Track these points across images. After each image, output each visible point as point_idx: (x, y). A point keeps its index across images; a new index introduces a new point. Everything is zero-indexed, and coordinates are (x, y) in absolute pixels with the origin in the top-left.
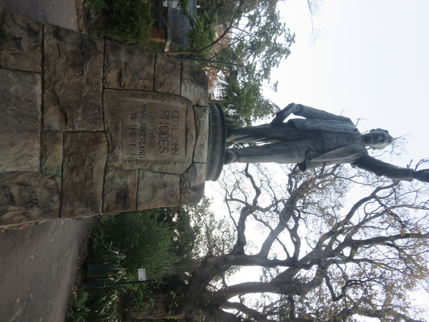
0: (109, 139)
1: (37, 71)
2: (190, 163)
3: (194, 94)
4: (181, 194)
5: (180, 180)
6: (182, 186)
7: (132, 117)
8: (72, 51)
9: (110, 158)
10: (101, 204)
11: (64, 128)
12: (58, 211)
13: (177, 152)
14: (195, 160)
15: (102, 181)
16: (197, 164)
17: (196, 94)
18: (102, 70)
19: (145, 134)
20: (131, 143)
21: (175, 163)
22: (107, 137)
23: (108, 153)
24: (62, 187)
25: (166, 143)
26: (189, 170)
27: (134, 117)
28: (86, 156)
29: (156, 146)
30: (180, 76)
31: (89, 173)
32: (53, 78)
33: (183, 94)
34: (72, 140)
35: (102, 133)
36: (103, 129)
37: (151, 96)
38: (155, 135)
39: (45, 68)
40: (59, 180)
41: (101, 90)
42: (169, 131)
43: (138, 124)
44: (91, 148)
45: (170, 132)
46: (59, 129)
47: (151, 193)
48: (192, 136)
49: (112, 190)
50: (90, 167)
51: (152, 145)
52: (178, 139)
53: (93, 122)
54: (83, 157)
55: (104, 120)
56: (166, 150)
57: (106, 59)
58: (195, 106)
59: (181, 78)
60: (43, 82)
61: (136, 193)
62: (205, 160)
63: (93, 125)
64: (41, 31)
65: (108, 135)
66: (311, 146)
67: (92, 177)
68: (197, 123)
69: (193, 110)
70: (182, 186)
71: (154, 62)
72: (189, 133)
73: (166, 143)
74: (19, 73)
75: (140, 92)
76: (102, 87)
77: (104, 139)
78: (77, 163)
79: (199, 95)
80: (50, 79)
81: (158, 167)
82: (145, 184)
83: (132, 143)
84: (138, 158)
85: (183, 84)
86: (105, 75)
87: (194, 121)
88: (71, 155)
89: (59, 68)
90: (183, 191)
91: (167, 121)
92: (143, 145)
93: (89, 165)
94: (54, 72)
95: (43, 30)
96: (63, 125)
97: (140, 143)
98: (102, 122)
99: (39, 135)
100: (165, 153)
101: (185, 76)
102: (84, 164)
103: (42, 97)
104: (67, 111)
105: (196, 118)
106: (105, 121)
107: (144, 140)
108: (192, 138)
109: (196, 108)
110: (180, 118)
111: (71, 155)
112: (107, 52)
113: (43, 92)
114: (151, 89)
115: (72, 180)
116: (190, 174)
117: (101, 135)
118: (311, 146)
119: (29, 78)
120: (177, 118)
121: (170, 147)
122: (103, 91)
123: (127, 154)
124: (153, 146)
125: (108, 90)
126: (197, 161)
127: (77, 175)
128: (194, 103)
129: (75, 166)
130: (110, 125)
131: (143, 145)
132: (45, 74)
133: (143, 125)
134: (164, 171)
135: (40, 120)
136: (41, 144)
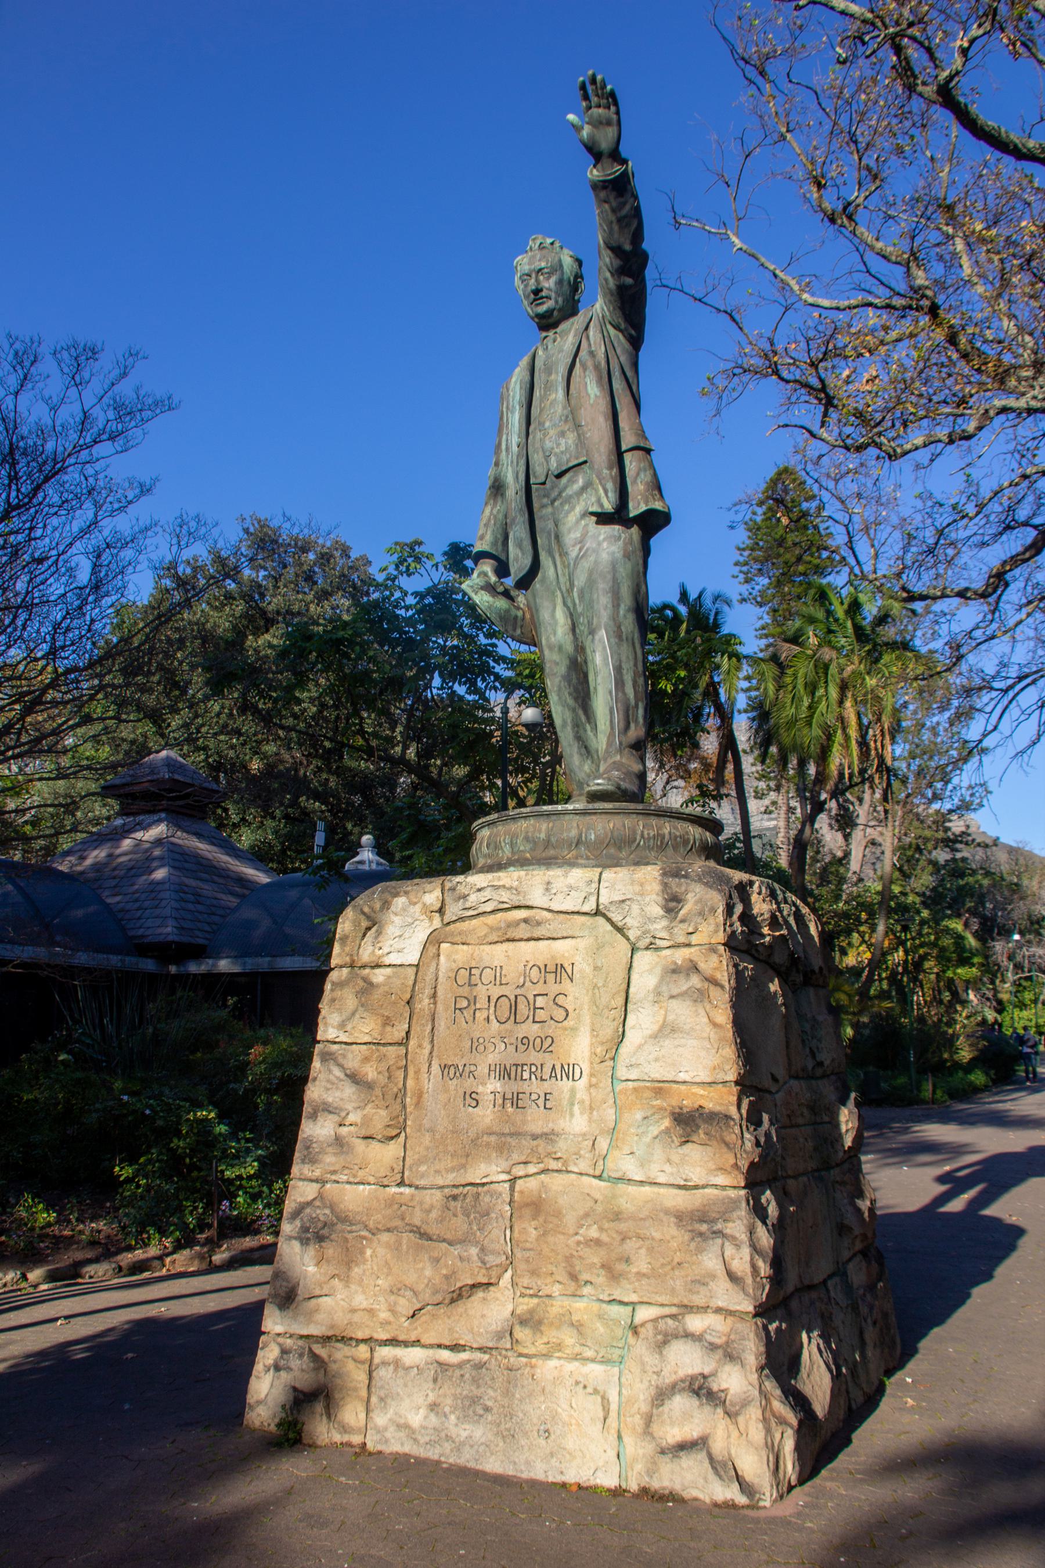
0: (532, 1169)
1: (368, 1355)
2: (601, 920)
4: (689, 945)
5: (647, 948)
7: (474, 1103)
8: (317, 1264)
9: (583, 1166)
10: (716, 1192)
11: (507, 1292)
12: (730, 1320)
13: (566, 965)
14: (590, 906)
15: (647, 1189)
16: (601, 901)
17: (410, 920)
18: (361, 1187)
19: (517, 1065)
20: (541, 1104)
22: (527, 1176)
23: (568, 1172)
24: (662, 1305)
25: (540, 1002)
26: (620, 924)
27: (473, 1098)
28: (577, 1234)
29: (550, 1032)
31: (623, 1226)
32: (384, 1315)
34: (534, 1273)
35: (517, 1188)
36: (507, 1185)
38: (521, 1036)
39: (360, 1335)
40: (644, 1314)
41: (407, 1190)
42: (507, 993)
43: (490, 1087)
44: (555, 1221)
45: (510, 991)
46: (510, 1307)
48: (517, 923)
49: (669, 1160)
50: (606, 1225)
51: (547, 1044)
53: (488, 1214)
54: (578, 1243)
55: (483, 1184)
56: (560, 1000)
57: (334, 1177)
59: (373, 967)
60: (393, 1342)
61: (683, 1087)
63: (493, 1215)
64: (280, 1340)
65: (521, 1173)
67: (633, 1218)
68: (489, 907)
69: (452, 926)
71: (336, 1047)
73: (540, 1002)
74: (374, 1399)
75: (410, 1083)
76: (402, 1189)
77: (532, 1184)
78: (596, 1260)
80: (385, 1323)
82: (656, 1060)
83: (541, 1102)
84: (582, 1084)
85: (387, 961)
86: (372, 1180)
88: (574, 1277)
89: (360, 1300)
90: (682, 939)
91: (482, 1003)
92: (547, 1070)
93: (601, 1229)
94: (371, 1312)
95: (279, 1335)
96: (499, 1295)
97: (542, 1080)
98: (486, 1188)
99: (524, 1360)
100: (568, 1003)
102: (598, 1242)
103: (431, 1346)
104: (459, 1285)
106: (484, 1180)
107: (534, 1069)
108: (526, 921)
109: (447, 918)
110: (473, 965)
111: (574, 1277)
112: (317, 1173)
113: (417, 1343)
114: (402, 1050)
115: (644, 1275)
117: (521, 1192)
119: (383, 1374)
120: (474, 971)
121: (553, 989)
122: (410, 1186)
123: (572, 1115)
125: (406, 1174)
126: (593, 899)
127: (627, 1260)
128: (437, 922)
129: (603, 1266)
130: (494, 1168)
131: (547, 1070)
132: (376, 1336)
133: (492, 1074)
134: (621, 1001)
135: (486, 1357)
136: (547, 1356)
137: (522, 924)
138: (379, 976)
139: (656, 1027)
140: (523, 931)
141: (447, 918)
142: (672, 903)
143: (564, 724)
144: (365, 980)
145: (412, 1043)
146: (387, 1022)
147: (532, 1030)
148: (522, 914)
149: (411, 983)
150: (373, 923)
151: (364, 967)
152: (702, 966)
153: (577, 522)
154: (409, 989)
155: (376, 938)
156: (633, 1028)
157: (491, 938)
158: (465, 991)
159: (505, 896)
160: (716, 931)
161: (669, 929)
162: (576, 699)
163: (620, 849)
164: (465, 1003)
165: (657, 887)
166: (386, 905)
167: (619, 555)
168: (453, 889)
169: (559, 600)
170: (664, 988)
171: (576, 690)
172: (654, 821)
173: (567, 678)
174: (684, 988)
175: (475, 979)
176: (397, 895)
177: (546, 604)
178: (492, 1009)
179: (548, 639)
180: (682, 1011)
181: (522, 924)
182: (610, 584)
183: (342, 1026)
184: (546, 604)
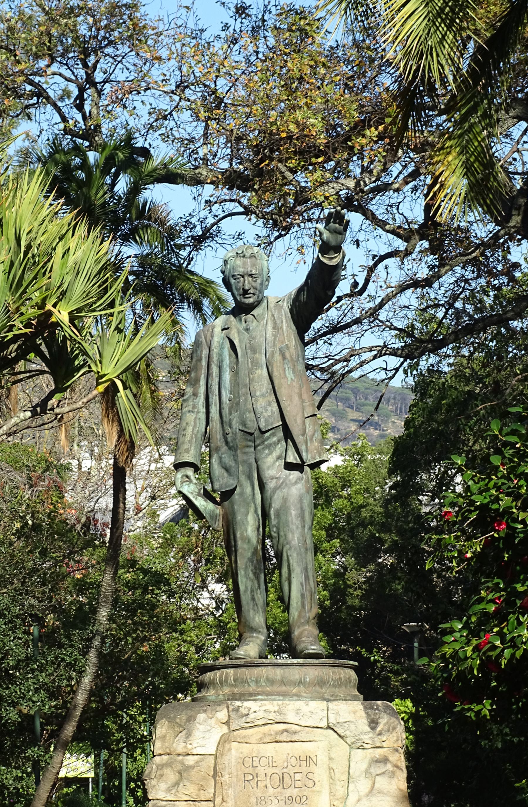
3: (209, 731)
6: (370, 746)
14: (324, 724)
16: (330, 721)
21: (331, 759)
25: (298, 777)
26: (342, 735)
29: (305, 794)
30: (180, 758)
37: (224, 804)
38: (287, 796)
47: (383, 798)
48: (282, 732)
52: (291, 755)
56: (310, 775)
58: (229, 728)
66: (275, 454)
68: (260, 722)
69: (237, 732)
70: (370, 746)
72: (278, 739)
73: (298, 777)
79: (210, 721)
81: (338, 788)
87: (256, 729)
90: (378, 744)
91: (262, 777)
101: (180, 750)
105: (250, 725)
108: (286, 731)
109: (233, 727)
116: (348, 733)
118: (275, 454)
121: (305, 769)
124: (305, 798)
134: (345, 777)
137: (287, 734)
138: (190, 761)
139: (367, 790)
140: (285, 737)
141: (233, 727)
142: (373, 724)
143: (246, 590)
144: (182, 763)
145: (218, 800)
146: (202, 788)
147: (294, 792)
149: (212, 765)
150: (185, 729)
152: (391, 758)
153: (274, 463)
154: (212, 769)
155: (187, 738)
156: (353, 791)
157: (265, 740)
158: (251, 770)
159: (272, 716)
160: (397, 740)
161: (372, 739)
162: (255, 574)
164: (251, 777)
165: (364, 715)
166: (191, 719)
167: (303, 491)
168: (237, 709)
169: (252, 510)
170: (372, 770)
171: (255, 568)
172: (336, 669)
173: (251, 560)
174: (384, 770)
175: (255, 764)
177: (242, 510)
178: (268, 780)
179: (242, 534)
180: (382, 783)
181: (287, 734)
182: (299, 512)
183: (168, 790)
184: (242, 510)
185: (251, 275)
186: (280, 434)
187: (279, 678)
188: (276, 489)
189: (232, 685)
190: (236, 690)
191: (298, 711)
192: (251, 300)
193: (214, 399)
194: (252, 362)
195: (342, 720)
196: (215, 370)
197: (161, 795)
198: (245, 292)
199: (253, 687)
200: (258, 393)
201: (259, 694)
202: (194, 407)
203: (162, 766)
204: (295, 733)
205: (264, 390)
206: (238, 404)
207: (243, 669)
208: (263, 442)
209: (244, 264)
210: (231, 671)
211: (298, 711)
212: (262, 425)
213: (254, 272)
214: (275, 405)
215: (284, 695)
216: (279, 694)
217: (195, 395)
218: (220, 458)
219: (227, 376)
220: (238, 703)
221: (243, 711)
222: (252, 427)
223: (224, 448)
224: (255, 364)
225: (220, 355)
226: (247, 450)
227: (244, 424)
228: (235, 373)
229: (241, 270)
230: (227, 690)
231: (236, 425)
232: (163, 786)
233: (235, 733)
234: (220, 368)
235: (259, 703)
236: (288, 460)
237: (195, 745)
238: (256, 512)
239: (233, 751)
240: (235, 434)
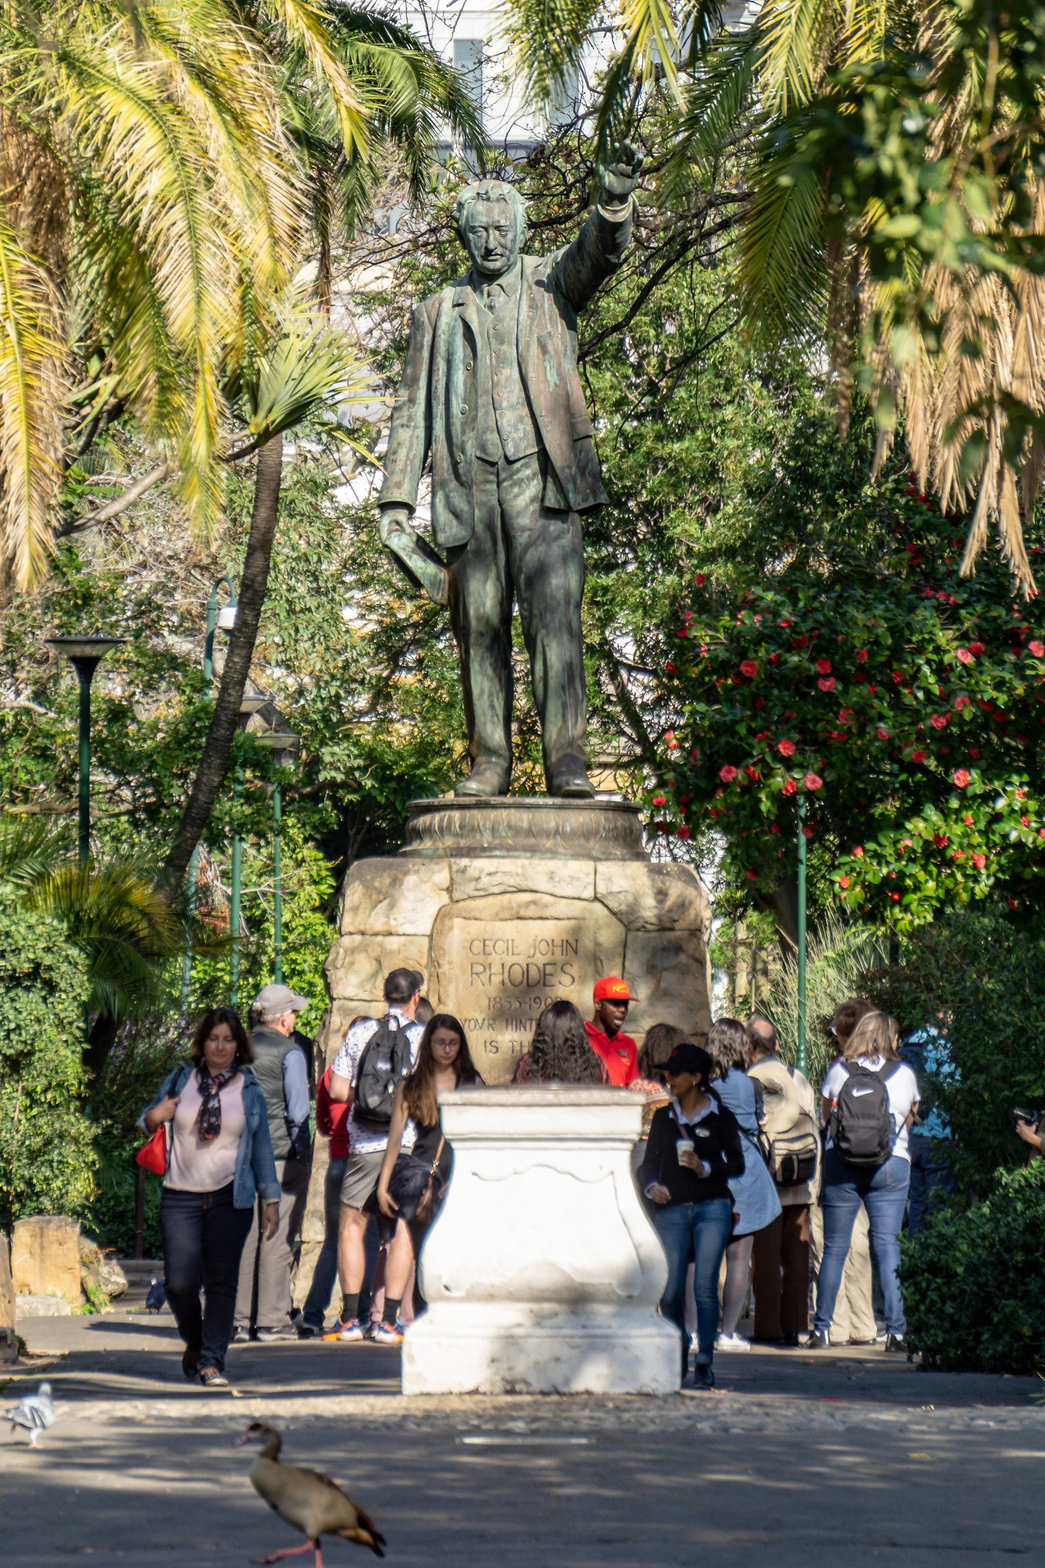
2: (598, 906)
14: (589, 893)
30: (380, 938)
33: (425, 927)
62: (588, 866)
68: (496, 890)
85: (400, 931)
87: (491, 899)
108: (534, 903)
109: (457, 895)
128: (445, 898)
141: (457, 895)
144: (381, 945)
148: (527, 897)
150: (385, 896)
151: (376, 934)
158: (481, 958)
163: (587, 839)
166: (396, 882)
168: (463, 871)
176: (406, 873)
183: (361, 985)
185: (498, 228)
186: (535, 465)
187: (525, 825)
188: (528, 546)
189: (457, 835)
190: (463, 843)
191: (551, 876)
192: (498, 264)
193: (439, 410)
194: (498, 357)
195: (615, 889)
196: (441, 365)
197: (350, 992)
198: (488, 253)
199: (486, 840)
200: (505, 404)
201: (495, 848)
202: (410, 419)
203: (353, 951)
204: (546, 906)
205: (514, 399)
206: (475, 418)
207: (475, 812)
208: (511, 477)
209: (489, 211)
210: (456, 815)
211: (551, 876)
212: (511, 452)
213: (503, 223)
214: (528, 421)
215: (533, 850)
216: (525, 849)
217: (412, 401)
218: (447, 498)
219: (460, 377)
220: (464, 862)
221: (472, 872)
222: (495, 454)
223: (454, 484)
224: (501, 360)
225: (450, 344)
226: (488, 486)
227: (483, 448)
228: (472, 372)
229: (483, 220)
230: (449, 841)
231: (471, 450)
232: (354, 979)
233: (461, 904)
234: (449, 363)
235: (495, 862)
236: (547, 504)
237: (401, 920)
238: (498, 578)
239: (456, 931)
240: (469, 463)
